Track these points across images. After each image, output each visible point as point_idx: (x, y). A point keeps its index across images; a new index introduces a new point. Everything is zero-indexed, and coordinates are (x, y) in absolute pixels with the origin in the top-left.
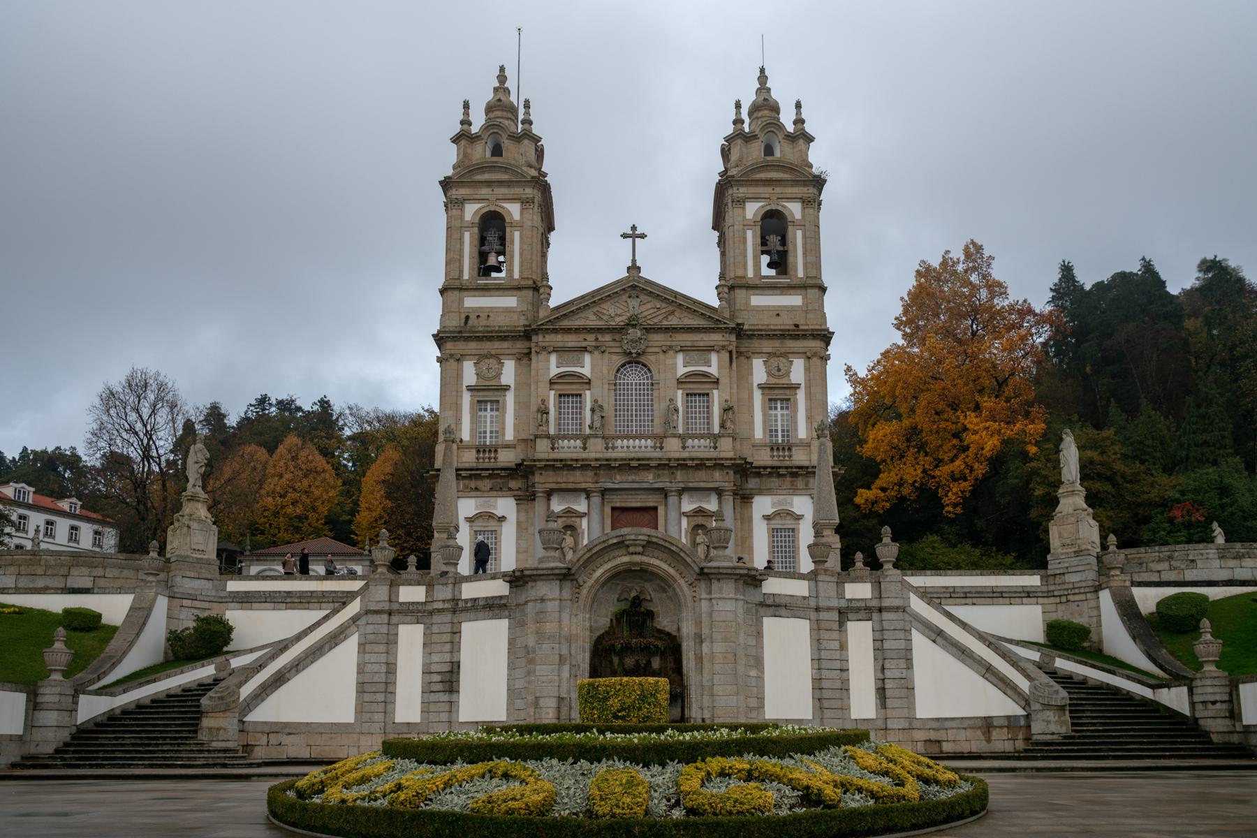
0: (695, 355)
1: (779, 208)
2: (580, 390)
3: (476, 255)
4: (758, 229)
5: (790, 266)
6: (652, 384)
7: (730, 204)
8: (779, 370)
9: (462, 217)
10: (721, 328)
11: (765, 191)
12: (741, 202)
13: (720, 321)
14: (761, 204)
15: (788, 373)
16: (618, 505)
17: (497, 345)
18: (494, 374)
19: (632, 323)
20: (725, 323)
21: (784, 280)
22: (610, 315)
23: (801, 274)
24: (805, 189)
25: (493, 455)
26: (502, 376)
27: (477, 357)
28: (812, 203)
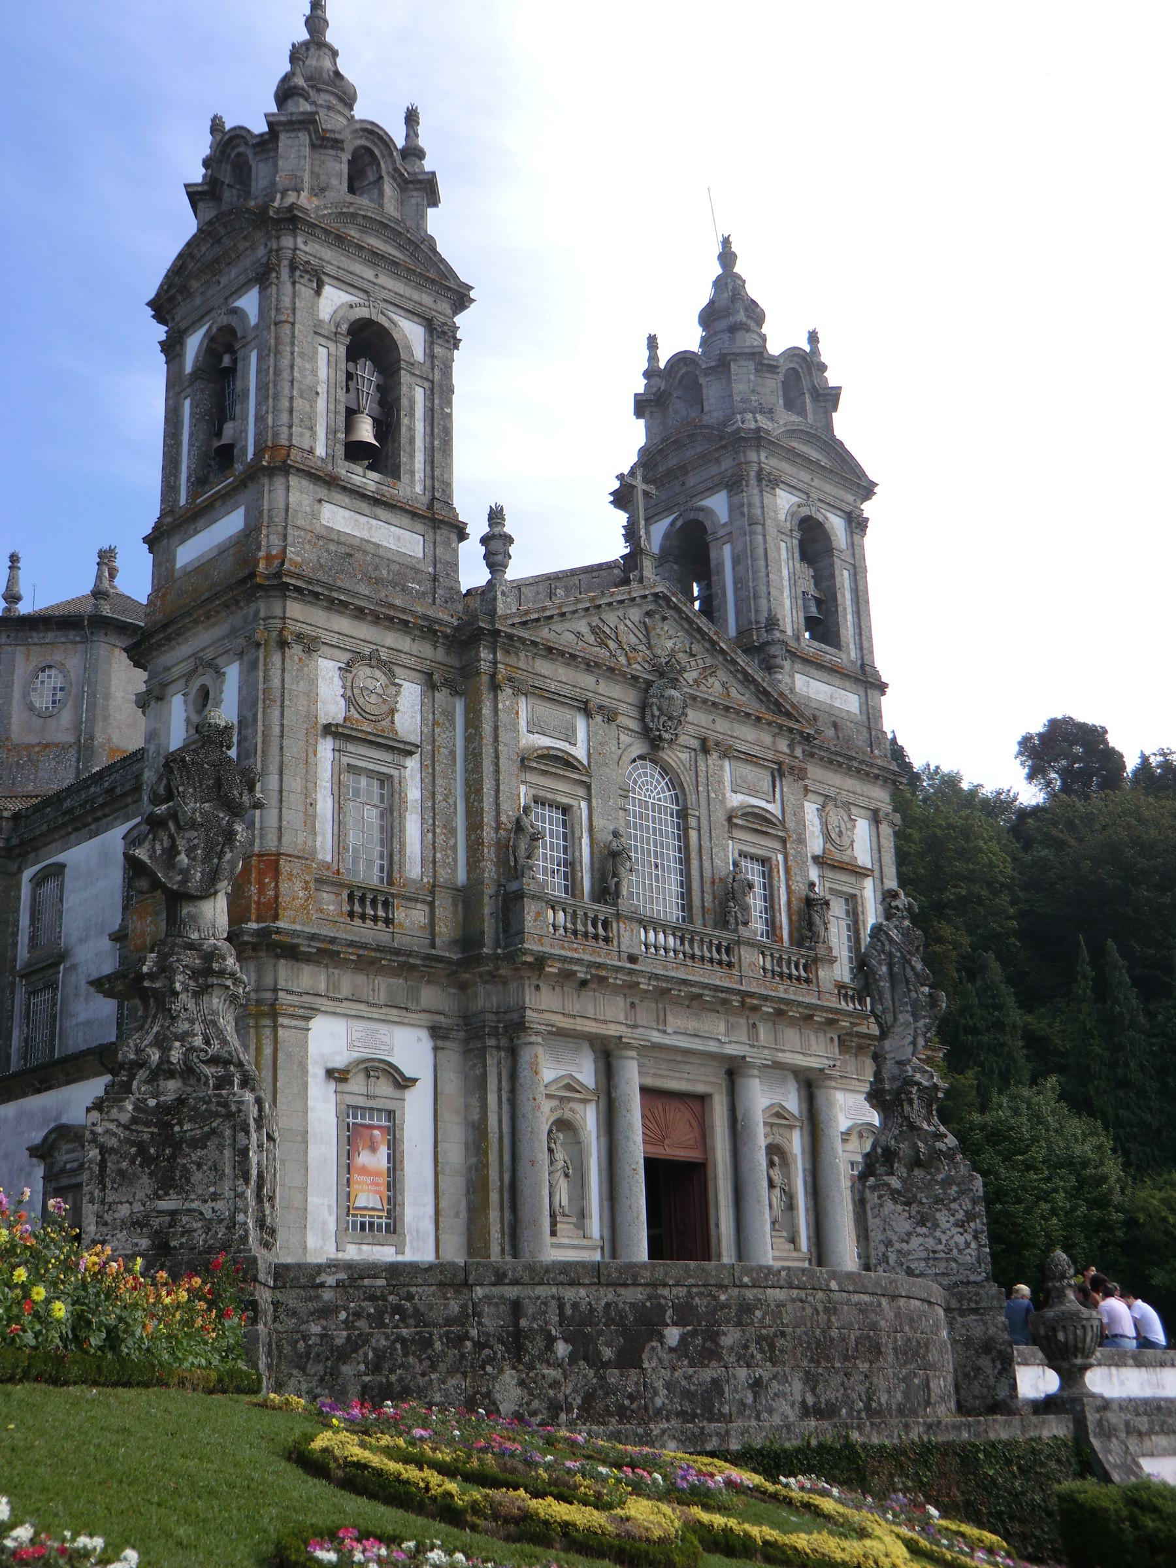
0: (747, 770)
1: (821, 519)
2: (574, 796)
4: (796, 542)
5: (842, 631)
7: (753, 482)
8: (840, 834)
9: (313, 309)
10: (791, 730)
11: (805, 476)
12: (770, 482)
13: (788, 715)
14: (795, 499)
16: (650, 1082)
17: (391, 639)
18: (385, 708)
19: (667, 672)
20: (798, 721)
21: (828, 653)
22: (620, 643)
23: (853, 655)
24: (850, 498)
25: (381, 913)
28: (857, 524)
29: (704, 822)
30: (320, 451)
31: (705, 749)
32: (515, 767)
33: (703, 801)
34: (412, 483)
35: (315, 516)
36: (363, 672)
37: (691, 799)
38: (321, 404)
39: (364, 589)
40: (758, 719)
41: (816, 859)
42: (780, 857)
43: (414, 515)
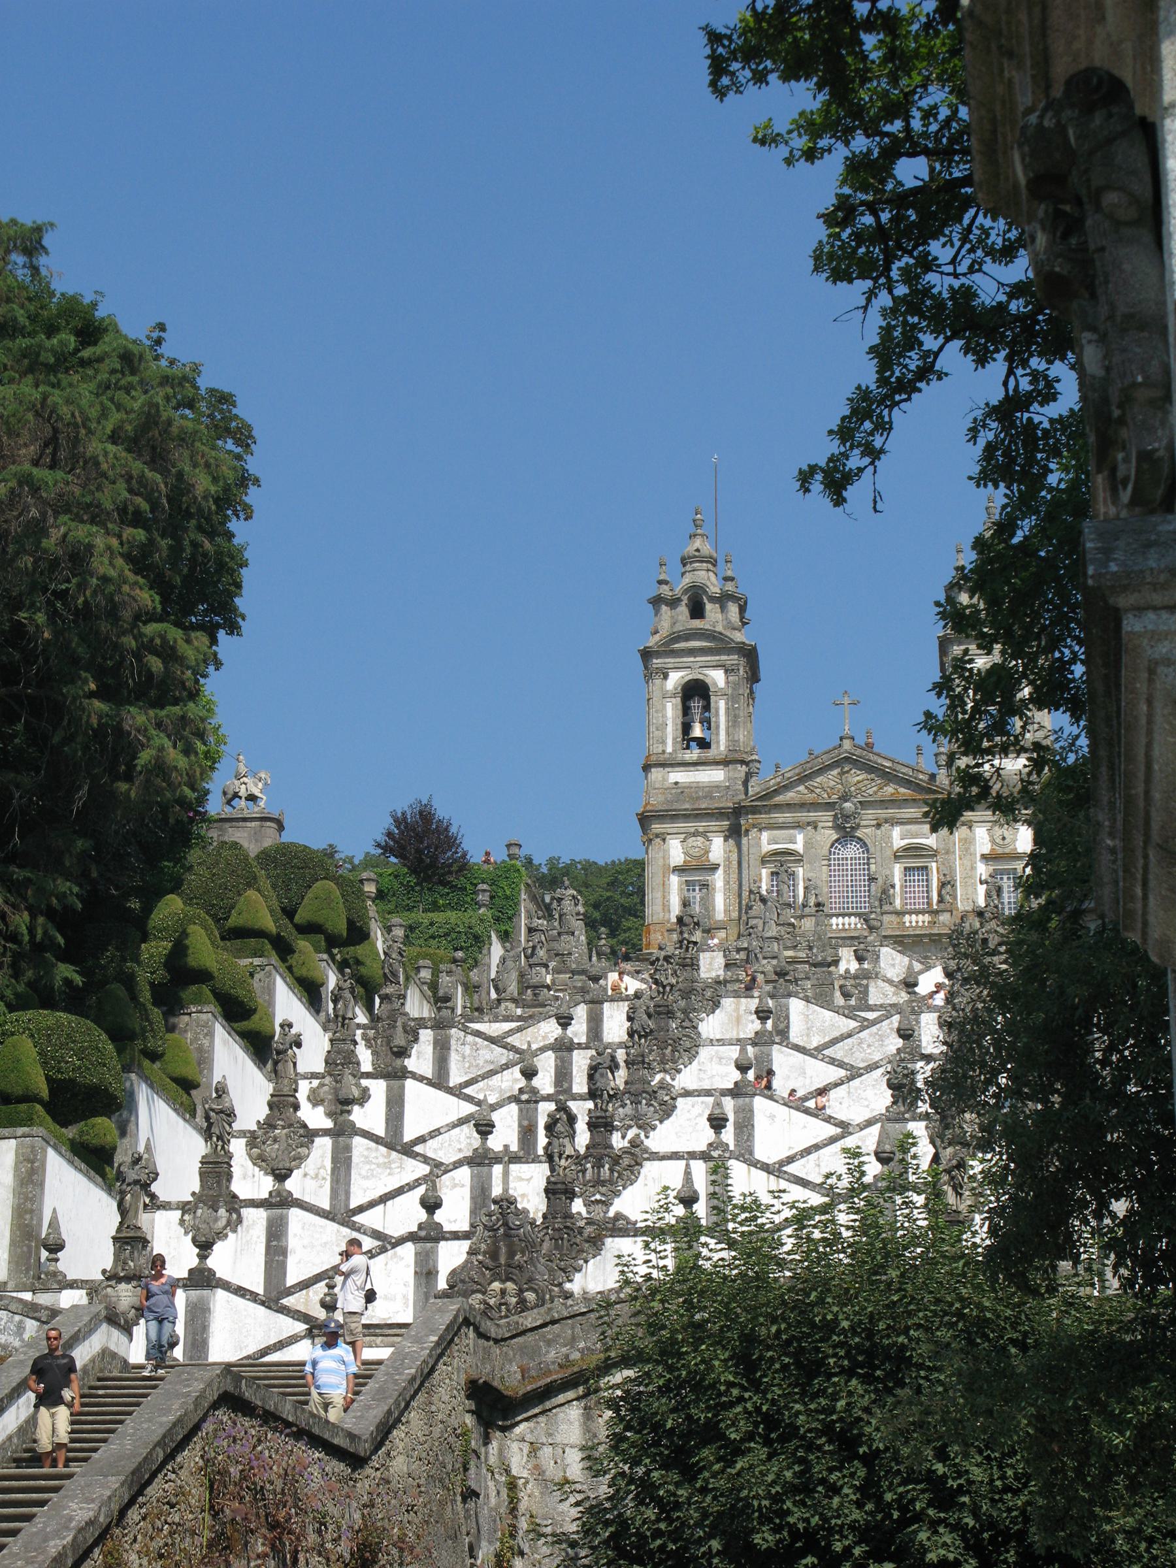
3: (680, 727)
6: (868, 859)
8: (1004, 839)
9: (662, 688)
15: (1015, 840)
26: (710, 855)
27: (683, 836)
29: (879, 859)
30: (669, 749)
31: (878, 826)
32: (759, 862)
33: (878, 848)
34: (718, 746)
35: (664, 780)
36: (691, 841)
37: (872, 850)
38: (670, 729)
39: (687, 806)
40: (914, 800)
41: (984, 857)
42: (934, 865)
43: (716, 763)
